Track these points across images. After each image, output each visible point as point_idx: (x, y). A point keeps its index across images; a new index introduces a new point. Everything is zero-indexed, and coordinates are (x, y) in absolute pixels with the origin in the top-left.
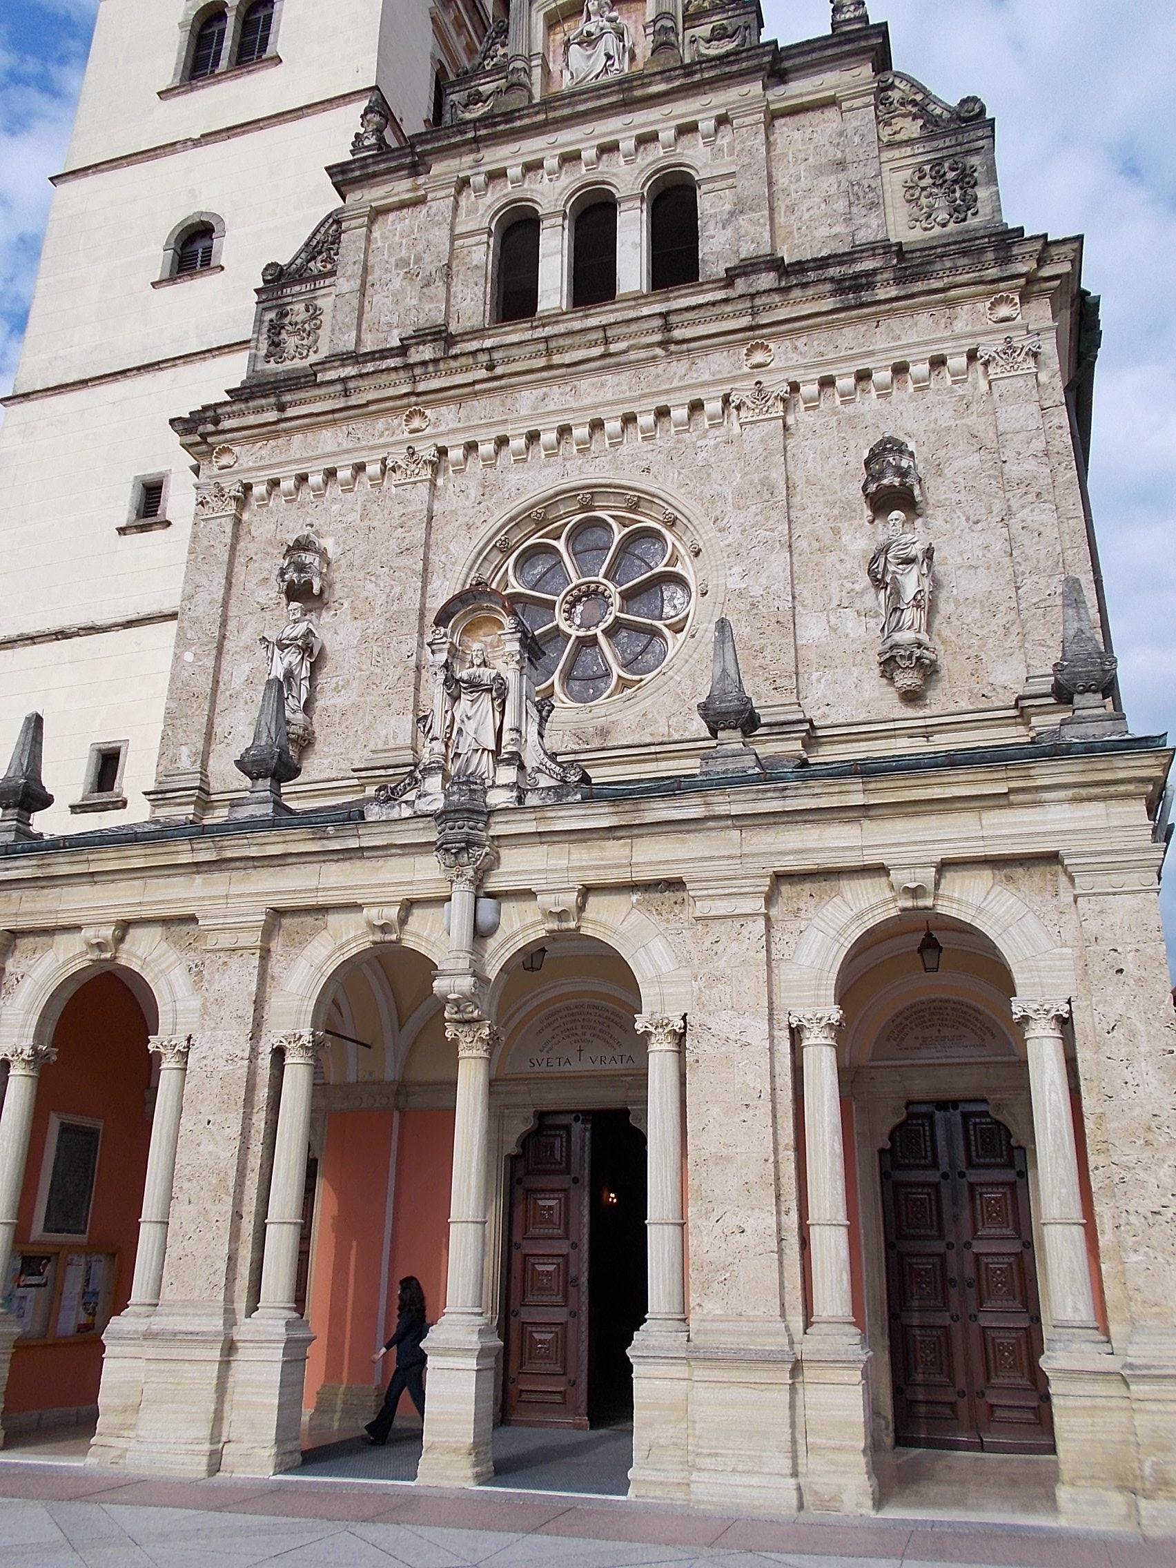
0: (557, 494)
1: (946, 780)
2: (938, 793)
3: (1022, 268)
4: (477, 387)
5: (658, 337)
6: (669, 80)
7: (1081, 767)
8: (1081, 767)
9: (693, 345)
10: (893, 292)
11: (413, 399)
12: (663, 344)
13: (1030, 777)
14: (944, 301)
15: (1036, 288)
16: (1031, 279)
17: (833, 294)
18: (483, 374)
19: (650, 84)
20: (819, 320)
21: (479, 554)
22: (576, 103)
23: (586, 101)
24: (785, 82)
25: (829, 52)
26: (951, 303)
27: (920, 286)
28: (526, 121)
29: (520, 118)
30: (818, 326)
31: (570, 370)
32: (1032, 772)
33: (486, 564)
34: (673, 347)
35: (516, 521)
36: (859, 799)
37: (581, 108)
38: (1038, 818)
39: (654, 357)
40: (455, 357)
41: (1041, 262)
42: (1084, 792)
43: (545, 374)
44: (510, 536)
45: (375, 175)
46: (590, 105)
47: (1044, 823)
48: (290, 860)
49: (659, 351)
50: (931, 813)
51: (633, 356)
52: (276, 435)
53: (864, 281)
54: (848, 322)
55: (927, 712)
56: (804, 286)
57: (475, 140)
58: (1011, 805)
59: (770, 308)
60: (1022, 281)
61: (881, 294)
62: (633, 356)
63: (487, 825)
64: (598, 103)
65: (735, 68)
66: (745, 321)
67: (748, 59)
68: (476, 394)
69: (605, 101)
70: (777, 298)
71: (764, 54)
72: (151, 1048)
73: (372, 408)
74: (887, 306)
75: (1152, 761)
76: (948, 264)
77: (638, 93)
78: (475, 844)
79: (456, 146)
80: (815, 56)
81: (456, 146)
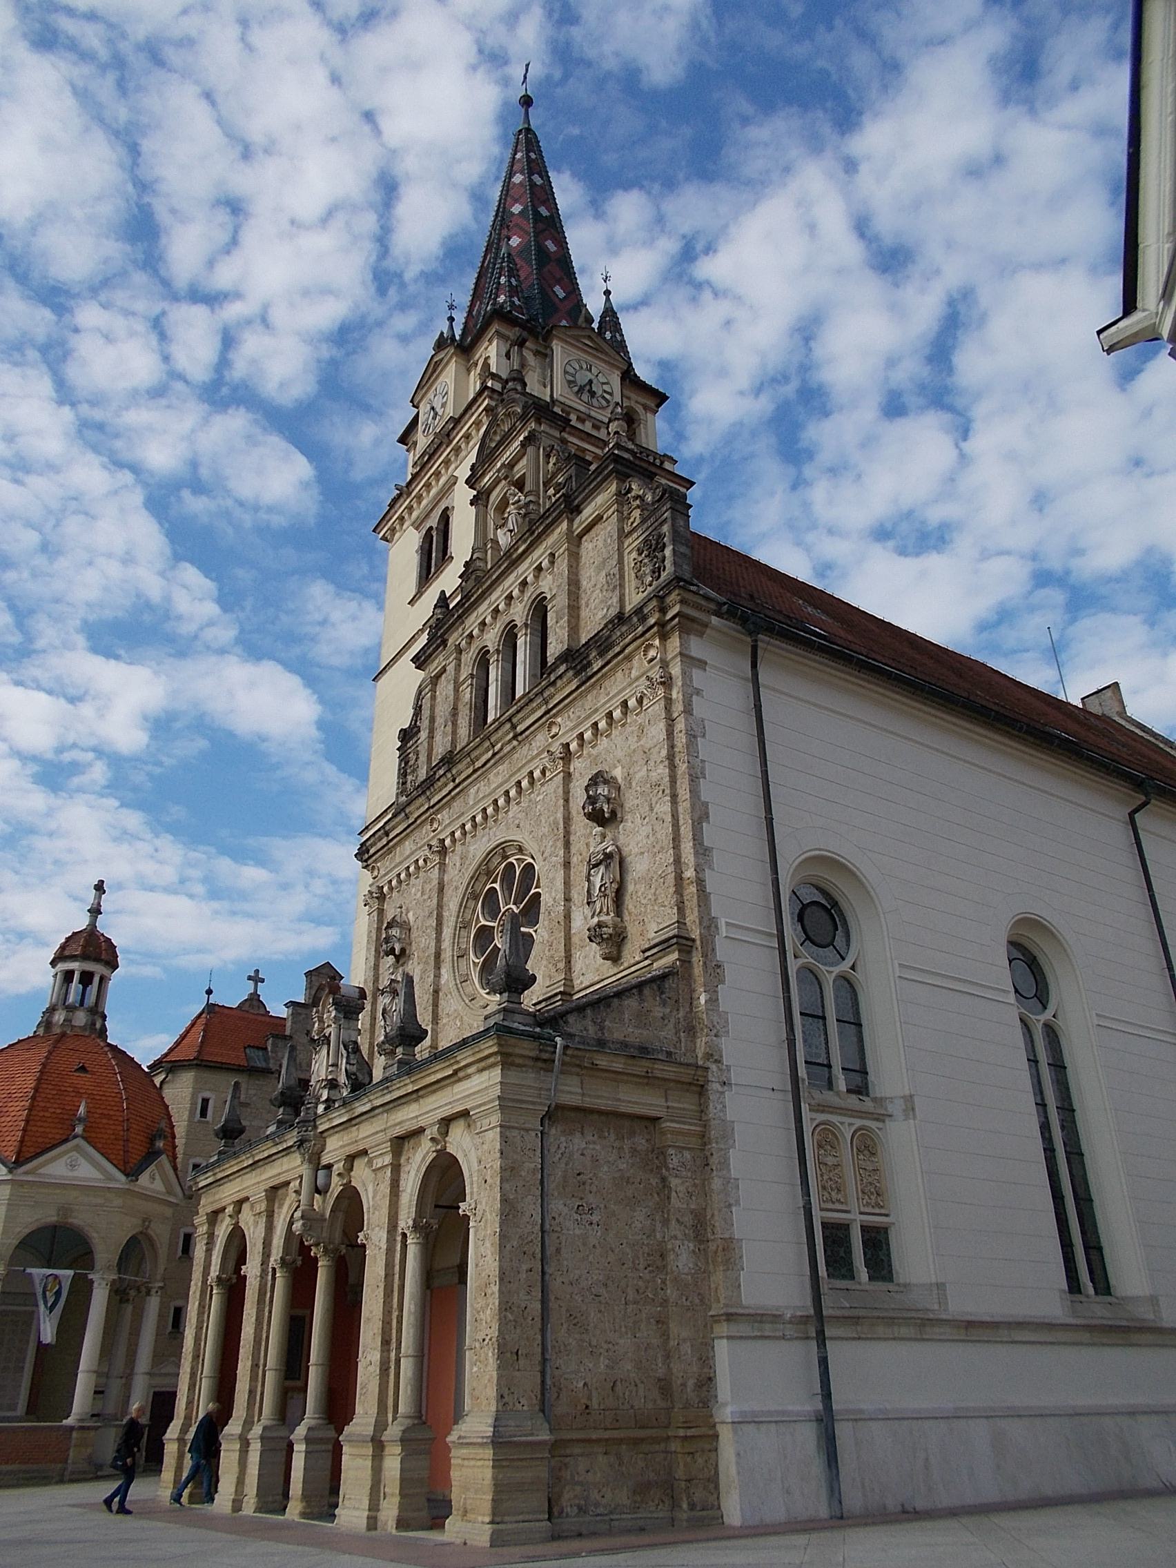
0: (488, 854)
1: (433, 1070)
2: (433, 1078)
3: (652, 621)
4: (453, 794)
5: (511, 735)
6: (525, 541)
7: (471, 1052)
8: (471, 1052)
9: (527, 733)
10: (600, 663)
11: (431, 811)
12: (515, 737)
13: (458, 1062)
14: (625, 658)
15: (669, 627)
16: (661, 624)
17: (576, 675)
18: (451, 785)
19: (517, 549)
20: (574, 695)
21: (461, 906)
22: (492, 575)
23: (495, 572)
24: (581, 512)
25: (599, 479)
26: (629, 658)
27: (611, 654)
28: (475, 596)
29: (472, 596)
30: (575, 699)
31: (484, 769)
32: (458, 1059)
33: (467, 911)
34: (520, 738)
35: (475, 878)
36: (410, 1088)
37: (494, 577)
38: (469, 1085)
39: (514, 747)
40: (438, 779)
41: (663, 610)
42: (483, 1064)
43: (475, 776)
44: (475, 887)
45: (430, 655)
46: (497, 574)
47: (471, 1088)
48: (274, 1158)
49: (515, 743)
50: (434, 1092)
51: (506, 750)
52: (390, 851)
53: (585, 662)
54: (588, 691)
55: (626, 965)
56: (560, 677)
57: (459, 617)
58: (460, 1080)
59: (552, 696)
60: (655, 629)
61: (596, 667)
62: (506, 750)
63: (315, 1127)
64: (500, 571)
65: (550, 519)
66: (544, 709)
67: (580, 493)
68: (453, 798)
69: (503, 568)
70: (552, 689)
71: (560, 505)
72: (242, 1273)
73: (418, 822)
74: (600, 675)
75: (491, 1043)
76: (619, 634)
77: (514, 556)
78: (306, 1141)
79: (453, 624)
80: (587, 491)
81: (453, 624)
